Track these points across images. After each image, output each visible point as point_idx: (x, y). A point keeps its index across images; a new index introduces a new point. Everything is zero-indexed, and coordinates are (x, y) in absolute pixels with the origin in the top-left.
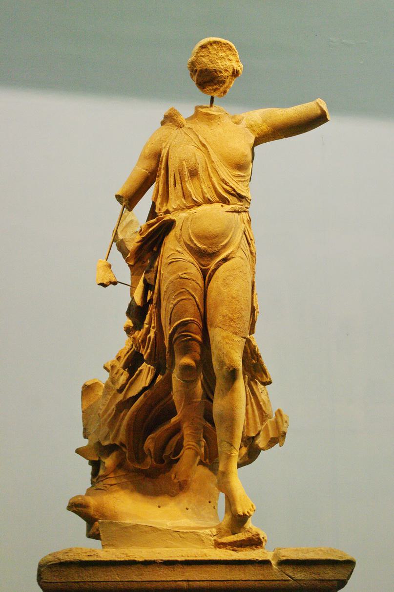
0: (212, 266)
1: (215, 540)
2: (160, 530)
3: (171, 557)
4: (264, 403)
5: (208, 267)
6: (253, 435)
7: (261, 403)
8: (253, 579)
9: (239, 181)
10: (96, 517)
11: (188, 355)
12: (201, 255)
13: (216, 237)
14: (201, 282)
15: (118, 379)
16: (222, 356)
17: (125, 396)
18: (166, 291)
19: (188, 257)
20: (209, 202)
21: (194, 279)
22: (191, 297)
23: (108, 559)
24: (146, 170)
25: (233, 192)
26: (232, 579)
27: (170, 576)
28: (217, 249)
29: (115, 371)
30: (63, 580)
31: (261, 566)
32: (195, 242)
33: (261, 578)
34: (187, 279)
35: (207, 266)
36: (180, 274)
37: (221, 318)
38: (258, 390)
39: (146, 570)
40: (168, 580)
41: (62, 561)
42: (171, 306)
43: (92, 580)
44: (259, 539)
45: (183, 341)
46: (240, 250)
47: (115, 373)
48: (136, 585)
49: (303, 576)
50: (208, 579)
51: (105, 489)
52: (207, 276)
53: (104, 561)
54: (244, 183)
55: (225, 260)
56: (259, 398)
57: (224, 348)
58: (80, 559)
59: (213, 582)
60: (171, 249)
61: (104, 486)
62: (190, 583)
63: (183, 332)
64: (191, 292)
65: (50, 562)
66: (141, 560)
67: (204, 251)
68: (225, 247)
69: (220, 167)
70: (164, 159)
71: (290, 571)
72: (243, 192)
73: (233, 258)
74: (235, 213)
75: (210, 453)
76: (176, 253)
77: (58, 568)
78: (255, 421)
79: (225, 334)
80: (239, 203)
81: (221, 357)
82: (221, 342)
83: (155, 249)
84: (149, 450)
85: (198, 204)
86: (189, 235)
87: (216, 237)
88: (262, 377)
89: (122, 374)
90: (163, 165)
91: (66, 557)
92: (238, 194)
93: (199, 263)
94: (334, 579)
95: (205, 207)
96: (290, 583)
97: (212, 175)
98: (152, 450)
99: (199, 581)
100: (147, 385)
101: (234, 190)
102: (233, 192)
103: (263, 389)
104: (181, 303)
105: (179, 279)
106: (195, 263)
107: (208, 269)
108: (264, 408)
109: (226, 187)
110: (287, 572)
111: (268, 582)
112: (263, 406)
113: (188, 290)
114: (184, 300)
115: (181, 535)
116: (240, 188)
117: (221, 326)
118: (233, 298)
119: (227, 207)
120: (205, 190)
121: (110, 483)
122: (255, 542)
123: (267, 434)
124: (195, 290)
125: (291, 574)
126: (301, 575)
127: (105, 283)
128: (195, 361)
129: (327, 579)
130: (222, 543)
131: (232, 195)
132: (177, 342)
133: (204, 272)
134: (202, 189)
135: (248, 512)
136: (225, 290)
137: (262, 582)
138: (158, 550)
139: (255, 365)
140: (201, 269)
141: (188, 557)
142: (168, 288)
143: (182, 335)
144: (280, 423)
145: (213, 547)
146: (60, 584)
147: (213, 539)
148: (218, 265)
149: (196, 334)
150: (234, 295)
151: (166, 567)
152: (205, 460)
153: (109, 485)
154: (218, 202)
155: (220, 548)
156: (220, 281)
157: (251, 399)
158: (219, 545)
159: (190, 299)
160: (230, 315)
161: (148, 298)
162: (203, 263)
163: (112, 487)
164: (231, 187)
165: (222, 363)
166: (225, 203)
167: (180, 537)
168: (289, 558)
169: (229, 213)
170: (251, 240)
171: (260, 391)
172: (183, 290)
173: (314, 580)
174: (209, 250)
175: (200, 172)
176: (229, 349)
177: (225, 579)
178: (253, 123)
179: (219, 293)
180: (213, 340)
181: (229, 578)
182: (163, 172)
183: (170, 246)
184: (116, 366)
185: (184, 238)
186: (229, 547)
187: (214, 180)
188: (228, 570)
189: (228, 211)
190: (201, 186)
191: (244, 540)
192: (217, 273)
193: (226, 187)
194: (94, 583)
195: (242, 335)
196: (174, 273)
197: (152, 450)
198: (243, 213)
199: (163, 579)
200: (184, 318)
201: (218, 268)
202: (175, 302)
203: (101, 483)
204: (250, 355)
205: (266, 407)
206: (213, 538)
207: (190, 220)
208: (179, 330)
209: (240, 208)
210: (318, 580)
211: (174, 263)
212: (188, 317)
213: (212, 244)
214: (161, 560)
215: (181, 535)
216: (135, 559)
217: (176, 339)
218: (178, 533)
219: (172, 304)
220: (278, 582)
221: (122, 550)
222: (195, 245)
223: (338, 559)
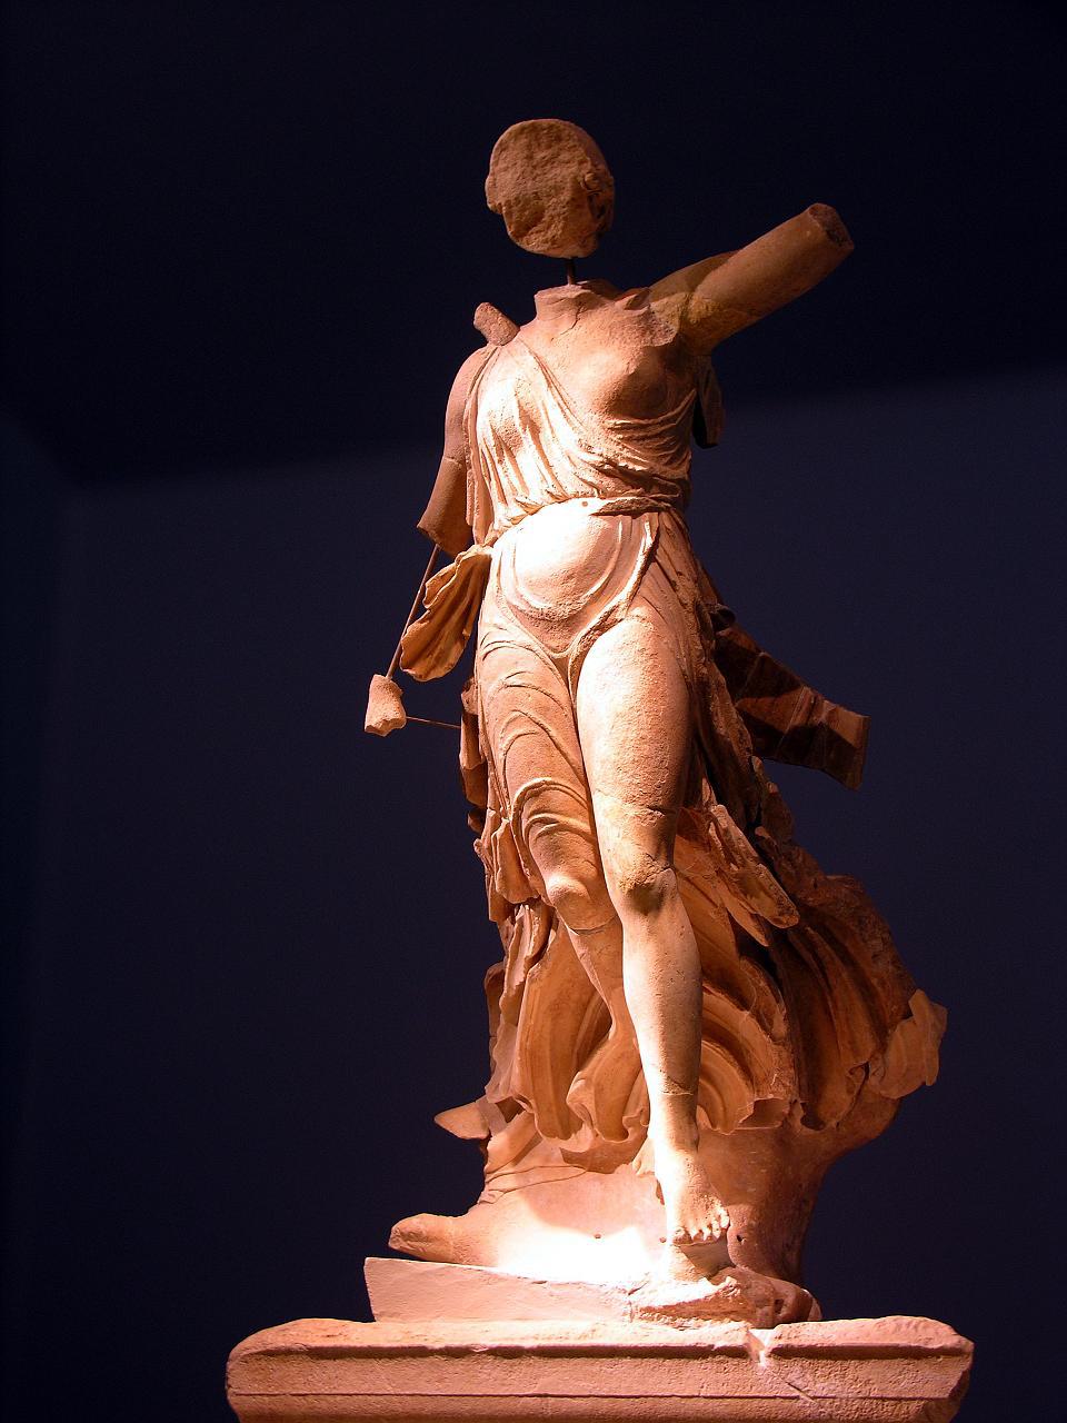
0: (574, 648)
2: (501, 1279)
5: (564, 654)
14: (559, 690)
17: (510, 987)
19: (519, 634)
21: (537, 686)
22: (537, 729)
28: (575, 606)
30: (271, 1390)
32: (528, 596)
35: (566, 647)
39: (451, 1369)
41: (269, 1347)
43: (334, 1392)
45: (540, 836)
48: (429, 1407)
49: (832, 1387)
51: (492, 1200)
52: (569, 672)
53: (355, 1348)
60: (488, 625)
64: (532, 713)
66: (438, 1346)
71: (795, 1370)
73: (616, 622)
75: (725, 1109)
76: (495, 629)
77: (263, 1363)
85: (532, 510)
91: (280, 1339)
93: (546, 645)
96: (800, 1403)
104: (516, 744)
105: (503, 690)
106: (536, 648)
107: (567, 658)
110: (792, 1377)
115: (553, 1290)
121: (502, 1188)
124: (544, 710)
125: (799, 1383)
128: (581, 880)
130: (649, 1310)
132: (532, 838)
133: (560, 664)
138: (489, 1326)
143: (535, 822)
146: (266, 1398)
149: (570, 816)
152: (713, 1125)
162: (554, 644)
172: (515, 714)
189: (597, 515)
194: (339, 1398)
195: (650, 802)
196: (494, 678)
197: (590, 1106)
201: (587, 652)
202: (503, 746)
208: (527, 810)
209: (633, 501)
211: (491, 654)
212: (536, 776)
213: (565, 595)
215: (553, 1290)
217: (529, 827)
221: (405, 1327)
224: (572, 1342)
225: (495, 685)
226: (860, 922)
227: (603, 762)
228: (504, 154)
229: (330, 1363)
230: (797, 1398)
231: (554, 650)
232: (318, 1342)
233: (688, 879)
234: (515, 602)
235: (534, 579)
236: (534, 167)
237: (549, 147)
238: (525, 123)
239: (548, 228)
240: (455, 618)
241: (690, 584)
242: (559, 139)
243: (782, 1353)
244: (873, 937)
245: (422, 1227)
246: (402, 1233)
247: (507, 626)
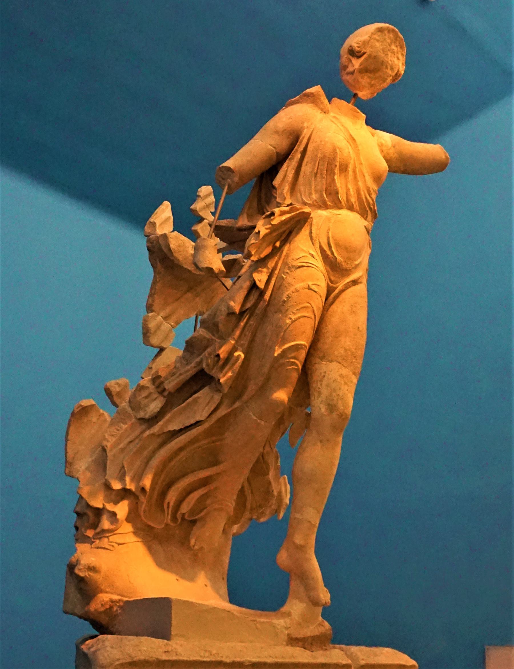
0: (340, 286)
3: (259, 657)
5: (335, 286)
10: (103, 587)
11: (285, 389)
12: (334, 267)
13: (355, 251)
15: (147, 406)
16: (335, 399)
18: (284, 301)
20: (351, 208)
22: (313, 317)
23: (192, 658)
24: (274, 148)
25: (372, 207)
29: (144, 394)
34: (315, 292)
36: (310, 283)
37: (342, 351)
41: (135, 659)
42: (288, 321)
47: (143, 395)
51: (111, 548)
52: (331, 296)
55: (355, 282)
57: (340, 389)
58: (157, 657)
61: (110, 545)
63: (293, 358)
65: (118, 660)
66: (228, 661)
67: (339, 263)
68: (357, 266)
70: (305, 141)
73: (361, 283)
76: (309, 256)
79: (344, 371)
81: (333, 400)
82: (339, 380)
83: (278, 244)
84: (169, 503)
86: (328, 238)
87: (355, 251)
89: (156, 399)
90: (301, 149)
95: (344, 213)
97: (359, 178)
98: (172, 504)
100: (202, 419)
101: (374, 205)
104: (301, 320)
107: (336, 288)
109: (368, 197)
113: (313, 306)
114: (306, 318)
117: (340, 361)
120: (352, 192)
124: (319, 308)
127: (214, 268)
131: (370, 209)
134: (348, 190)
136: (351, 319)
140: (328, 285)
141: (276, 657)
142: (289, 297)
148: (347, 287)
153: (116, 543)
154: (358, 213)
156: (346, 308)
159: (311, 318)
160: (354, 350)
161: (248, 305)
162: (333, 278)
163: (120, 546)
165: (331, 407)
166: (363, 217)
167: (257, 629)
172: (308, 305)
174: (344, 265)
175: (350, 169)
176: (347, 392)
178: (383, 142)
179: (343, 321)
180: (324, 376)
182: (299, 156)
183: (301, 246)
184: (148, 387)
185: (321, 240)
187: (360, 184)
190: (347, 186)
192: (343, 295)
193: (368, 197)
196: (303, 281)
197: (172, 504)
200: (299, 340)
202: (293, 317)
203: (106, 540)
206: (286, 632)
207: (332, 221)
211: (305, 268)
212: (302, 340)
213: (349, 258)
214: (250, 661)
216: (224, 659)
218: (255, 622)
219: (291, 319)
222: (332, 253)
225: (302, 285)
227: (346, 350)
228: (379, 33)
231: (331, 281)
234: (326, 248)
235: (341, 243)
236: (389, 50)
238: (391, 26)
239: (375, 79)
240: (275, 234)
246: (89, 567)
247: (317, 258)
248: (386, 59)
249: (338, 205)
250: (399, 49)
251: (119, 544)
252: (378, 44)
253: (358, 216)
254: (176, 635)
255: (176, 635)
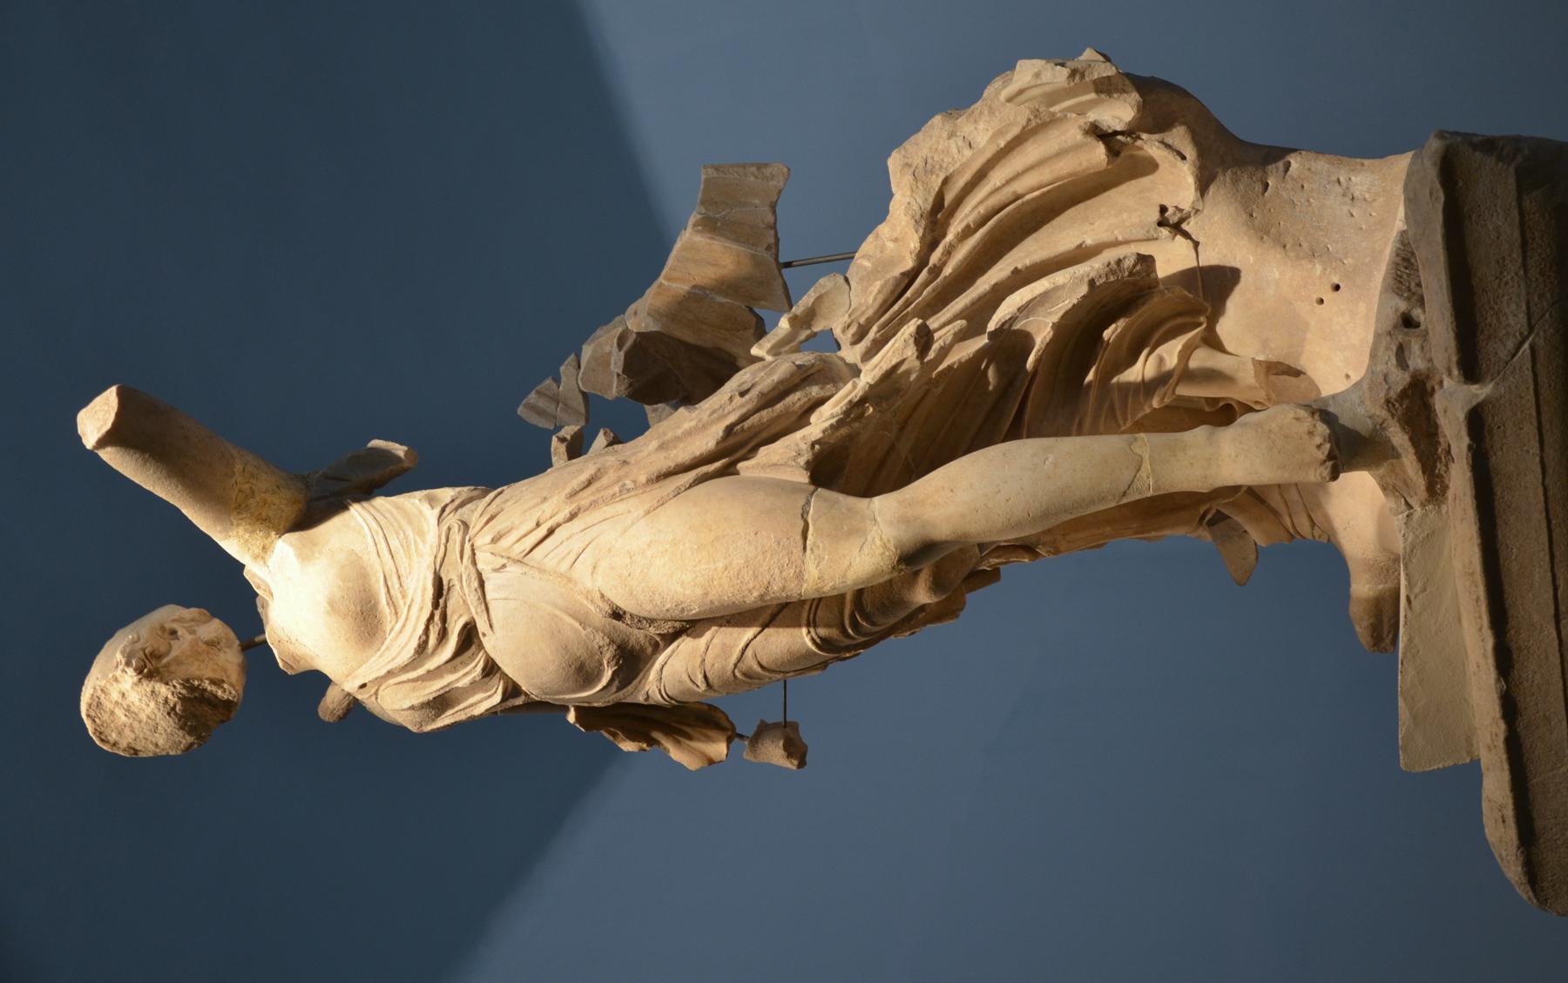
1: (1423, 505)
4: (1000, 133)
6: (1099, 152)
7: (1002, 144)
8: (1535, 449)
9: (404, 597)
20: (491, 669)
22: (749, 652)
25: (437, 618)
26: (1541, 506)
27: (1547, 658)
31: (1490, 432)
33: (1530, 429)
34: (705, 677)
38: (964, 166)
40: (1558, 661)
44: (1403, 394)
46: (575, 574)
49: (1513, 307)
50: (1547, 566)
54: (402, 571)
56: (988, 154)
59: (1557, 554)
62: (1562, 608)
69: (394, 652)
71: (1496, 349)
72: (424, 589)
73: (603, 596)
74: (488, 597)
75: (1180, 314)
78: (1060, 154)
80: (458, 587)
88: (908, 373)
92: (436, 605)
94: (1515, 212)
96: (1541, 342)
97: (421, 671)
99: (1556, 589)
102: (437, 618)
103: (960, 143)
108: (1015, 131)
110: (1503, 354)
111: (1544, 408)
112: (1009, 137)
113: (731, 666)
115: (1417, 590)
116: (418, 599)
118: (706, 594)
119: (482, 626)
122: (1414, 403)
123: (1092, 104)
125: (1510, 344)
126: (1511, 313)
129: (1517, 234)
130: (1431, 489)
131: (444, 619)
135: (1319, 447)
137: (1546, 426)
139: (876, 405)
144: (1047, 89)
145: (1444, 508)
147: (1418, 508)
150: (699, 592)
151: (1517, 666)
155: (1445, 488)
157: (997, 190)
158: (1436, 489)
162: (649, 650)
164: (427, 631)
168: (1454, 359)
169: (494, 621)
170: (538, 525)
171: (968, 153)
173: (1526, 272)
177: (1544, 525)
181: (1538, 517)
186: (1440, 467)
188: (1512, 518)
191: (1411, 439)
195: (798, 550)
198: (480, 567)
199: (1558, 671)
204: (856, 425)
205: (1010, 125)
206: (1418, 508)
210: (1525, 258)
214: (1498, 681)
215: (1417, 590)
216: (1502, 737)
220: (1542, 379)
223: (1440, 206)
224: (1481, 591)
226: (932, 172)
229: (1539, 824)
230: (1532, 348)
232: (1511, 833)
233: (902, 429)
237: (112, 713)
241: (548, 508)
242: (99, 704)
243: (1471, 369)
244: (947, 151)
245: (1365, 623)
248: (159, 715)
249: (512, 690)
250: (108, 705)
251: (1313, 524)
252: (161, 742)
253: (488, 642)
254: (1469, 753)
255: (1469, 753)
